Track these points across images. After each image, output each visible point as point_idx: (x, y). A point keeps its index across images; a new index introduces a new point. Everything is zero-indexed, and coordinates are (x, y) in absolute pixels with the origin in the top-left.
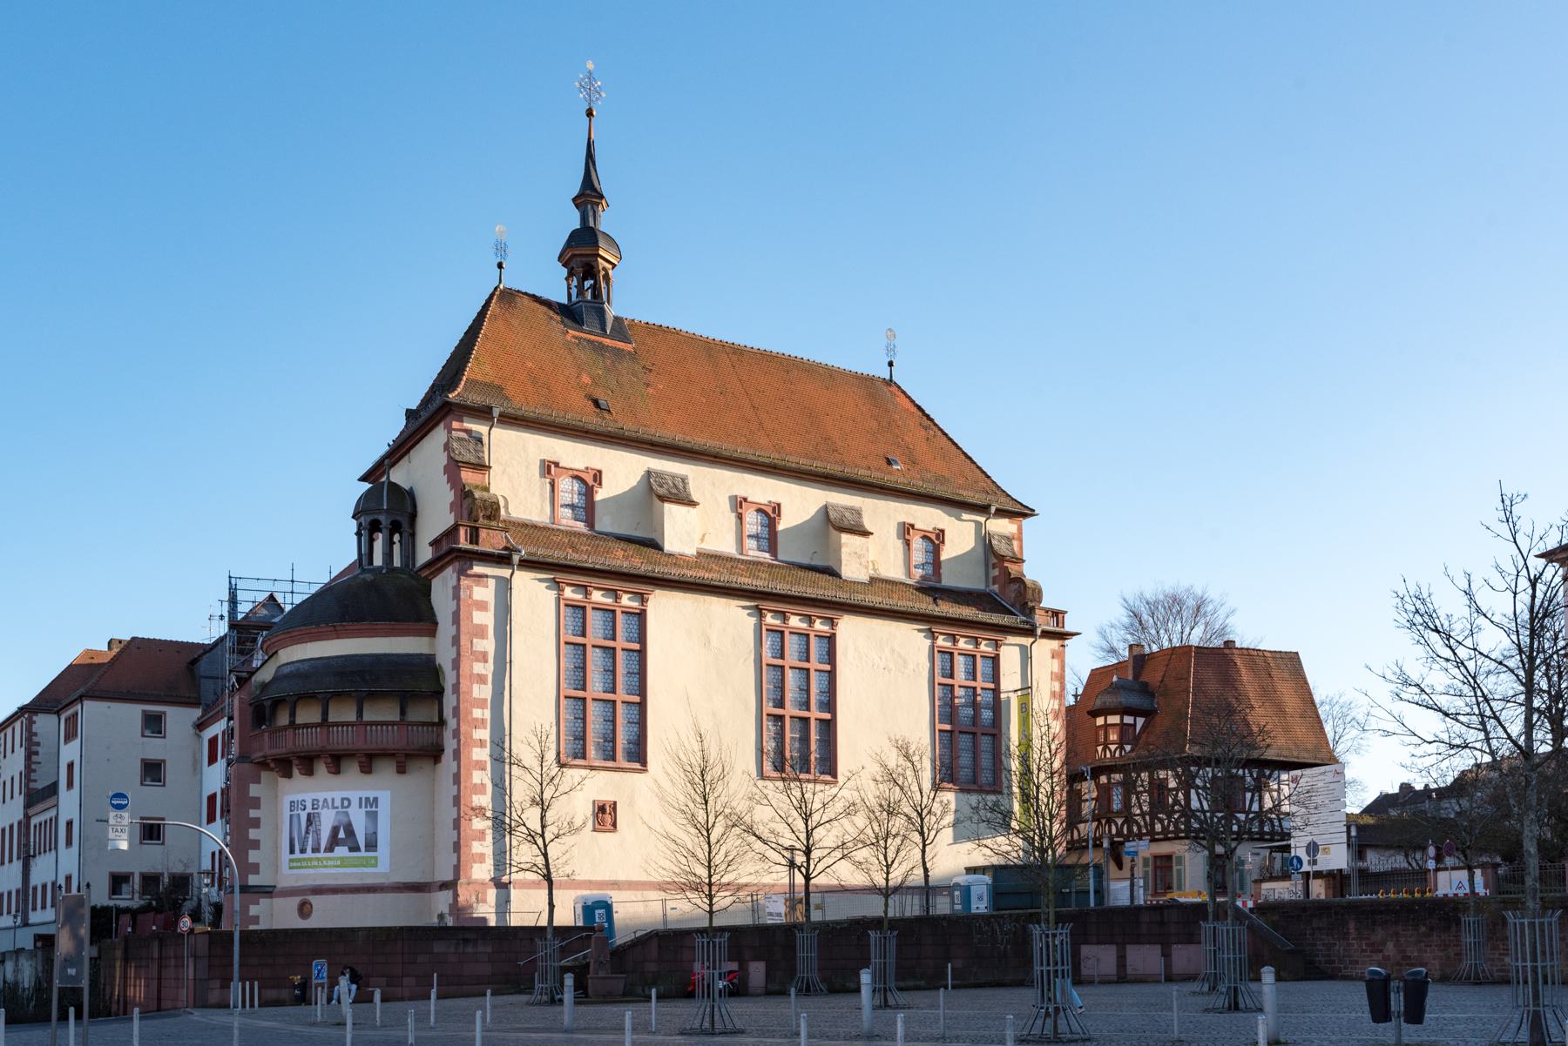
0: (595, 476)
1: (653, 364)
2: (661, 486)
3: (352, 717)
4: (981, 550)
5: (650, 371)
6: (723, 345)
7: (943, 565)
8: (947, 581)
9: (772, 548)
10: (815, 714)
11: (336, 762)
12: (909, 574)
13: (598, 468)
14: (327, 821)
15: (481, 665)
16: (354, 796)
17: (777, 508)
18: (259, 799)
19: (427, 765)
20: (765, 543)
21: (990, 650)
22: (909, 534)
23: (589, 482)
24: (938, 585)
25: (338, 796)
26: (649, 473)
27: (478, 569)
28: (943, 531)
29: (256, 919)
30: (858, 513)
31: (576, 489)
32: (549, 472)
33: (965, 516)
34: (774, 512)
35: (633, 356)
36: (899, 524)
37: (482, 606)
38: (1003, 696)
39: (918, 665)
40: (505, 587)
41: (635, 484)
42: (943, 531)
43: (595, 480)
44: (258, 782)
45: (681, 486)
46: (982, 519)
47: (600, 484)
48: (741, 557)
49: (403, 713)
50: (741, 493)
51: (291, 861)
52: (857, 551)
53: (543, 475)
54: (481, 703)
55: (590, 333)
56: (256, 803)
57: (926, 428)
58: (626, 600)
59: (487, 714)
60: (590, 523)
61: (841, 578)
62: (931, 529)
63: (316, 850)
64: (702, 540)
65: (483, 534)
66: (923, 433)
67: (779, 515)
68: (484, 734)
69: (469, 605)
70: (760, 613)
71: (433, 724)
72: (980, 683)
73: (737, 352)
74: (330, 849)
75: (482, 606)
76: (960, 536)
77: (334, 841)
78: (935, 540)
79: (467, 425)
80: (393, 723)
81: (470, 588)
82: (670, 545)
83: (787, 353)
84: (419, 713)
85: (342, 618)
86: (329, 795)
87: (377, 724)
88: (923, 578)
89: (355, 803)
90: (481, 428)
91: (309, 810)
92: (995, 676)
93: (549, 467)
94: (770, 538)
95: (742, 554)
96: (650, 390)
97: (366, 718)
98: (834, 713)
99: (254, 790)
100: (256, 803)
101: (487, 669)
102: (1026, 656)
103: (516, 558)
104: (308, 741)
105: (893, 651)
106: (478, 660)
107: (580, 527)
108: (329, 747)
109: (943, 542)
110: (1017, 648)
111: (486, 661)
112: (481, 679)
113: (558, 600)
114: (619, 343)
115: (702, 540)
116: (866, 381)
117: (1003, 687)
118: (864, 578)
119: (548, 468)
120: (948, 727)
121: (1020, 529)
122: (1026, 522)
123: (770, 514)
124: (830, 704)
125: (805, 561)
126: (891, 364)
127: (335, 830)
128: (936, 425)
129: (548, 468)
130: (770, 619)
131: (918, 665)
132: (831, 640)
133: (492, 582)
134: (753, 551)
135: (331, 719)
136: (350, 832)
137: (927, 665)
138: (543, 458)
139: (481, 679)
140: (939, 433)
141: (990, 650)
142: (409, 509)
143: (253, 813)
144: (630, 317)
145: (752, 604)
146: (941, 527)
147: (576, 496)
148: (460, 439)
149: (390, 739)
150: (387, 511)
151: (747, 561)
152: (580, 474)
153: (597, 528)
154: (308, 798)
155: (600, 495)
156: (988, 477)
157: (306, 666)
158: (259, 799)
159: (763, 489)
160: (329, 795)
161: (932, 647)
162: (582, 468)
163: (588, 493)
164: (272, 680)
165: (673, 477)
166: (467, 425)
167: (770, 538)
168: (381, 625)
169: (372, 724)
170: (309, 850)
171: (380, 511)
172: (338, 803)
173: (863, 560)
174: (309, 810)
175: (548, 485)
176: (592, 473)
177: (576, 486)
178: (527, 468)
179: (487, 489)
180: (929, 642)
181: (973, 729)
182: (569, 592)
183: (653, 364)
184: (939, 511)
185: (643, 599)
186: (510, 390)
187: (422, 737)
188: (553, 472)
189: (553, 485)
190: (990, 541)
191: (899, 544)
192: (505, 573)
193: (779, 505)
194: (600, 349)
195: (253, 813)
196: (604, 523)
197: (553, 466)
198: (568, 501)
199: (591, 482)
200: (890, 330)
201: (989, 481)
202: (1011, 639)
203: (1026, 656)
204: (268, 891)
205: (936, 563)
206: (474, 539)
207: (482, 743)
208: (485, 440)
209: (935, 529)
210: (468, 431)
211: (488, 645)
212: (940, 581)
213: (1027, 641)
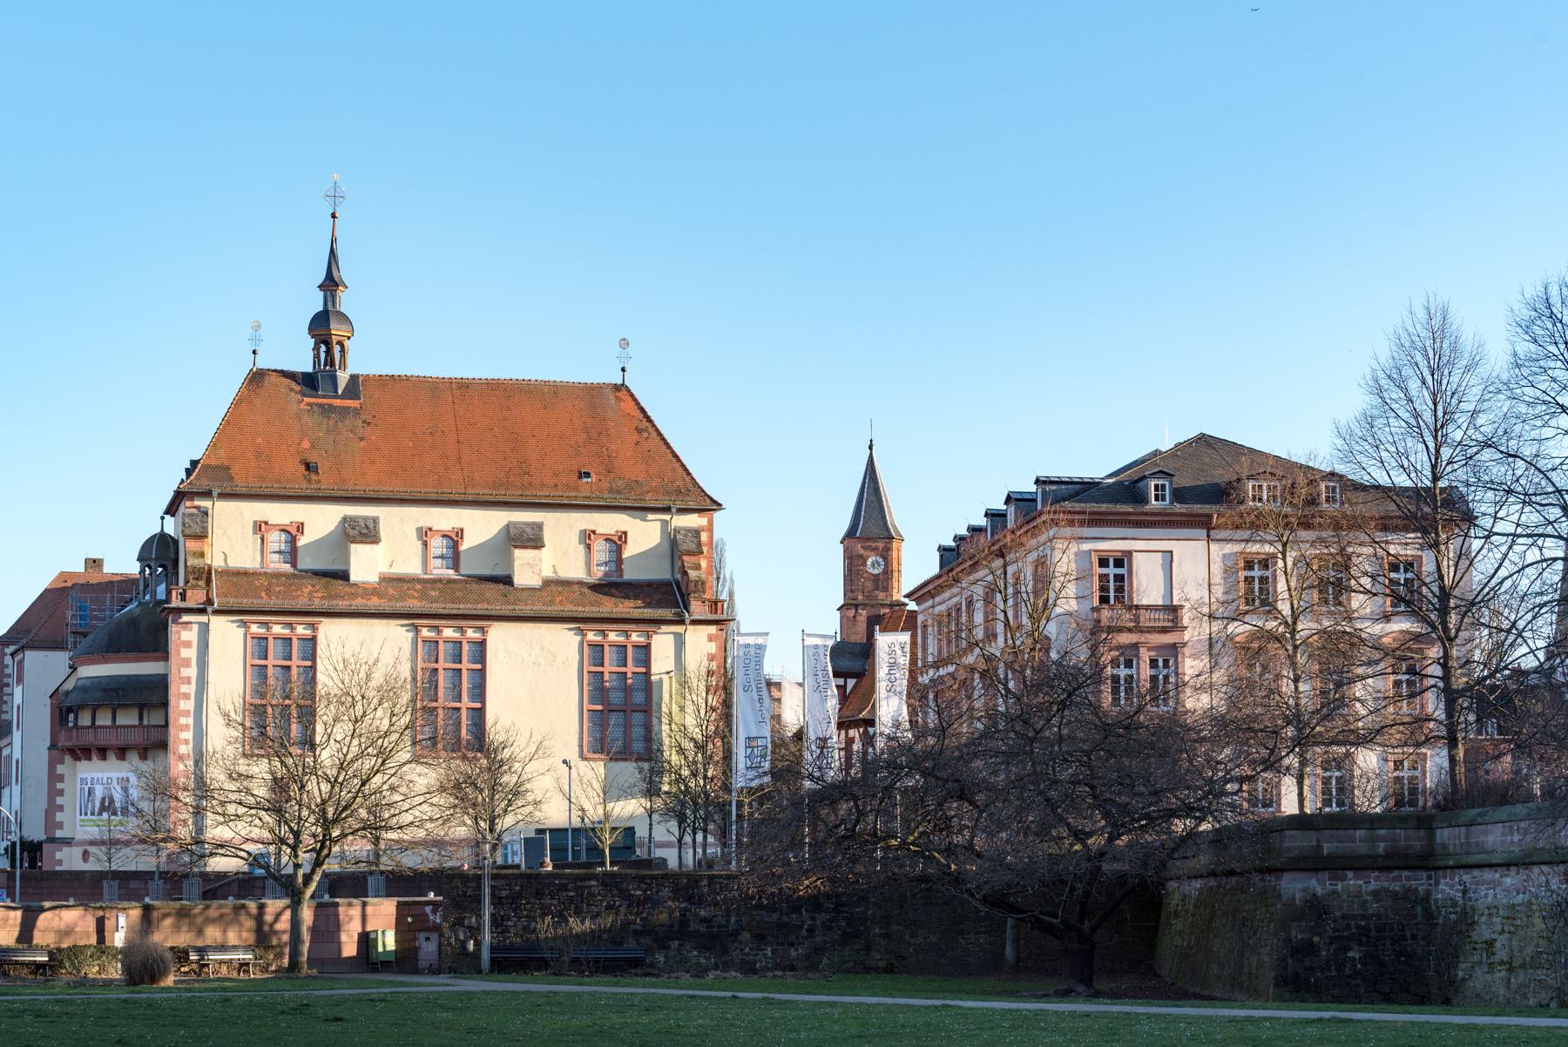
0: (298, 527)
1: (374, 417)
2: (354, 529)
3: (108, 722)
4: (667, 546)
5: (369, 424)
6: (450, 382)
7: (625, 562)
8: (629, 575)
9: (456, 567)
10: (466, 702)
11: (103, 753)
12: (589, 573)
13: (301, 521)
14: (99, 792)
15: (186, 686)
16: (115, 775)
17: (460, 533)
18: (63, 775)
19: (160, 753)
20: (450, 562)
21: (642, 639)
22: (590, 538)
23: (293, 533)
24: (619, 580)
25: (105, 775)
26: (345, 519)
27: (185, 618)
28: (625, 533)
29: (60, 862)
30: (539, 527)
31: (283, 539)
32: (260, 530)
33: (650, 516)
34: (457, 536)
35: (357, 412)
36: (581, 531)
37: (188, 644)
38: (653, 678)
39: (567, 658)
40: (205, 629)
41: (333, 528)
42: (625, 533)
43: (298, 531)
44: (63, 763)
45: (371, 526)
46: (667, 517)
47: (302, 533)
48: (425, 577)
49: (141, 719)
50: (425, 523)
51: (81, 820)
52: (531, 562)
53: (255, 533)
54: (186, 714)
55: (324, 397)
56: (61, 778)
57: (639, 430)
58: (300, 630)
59: (190, 721)
60: (294, 565)
61: (513, 586)
62: (613, 533)
63: (93, 814)
64: (391, 566)
65: (189, 593)
66: (635, 437)
67: (462, 538)
68: (188, 735)
69: (178, 645)
70: (416, 629)
71: (161, 726)
72: (631, 668)
73: (463, 386)
74: (100, 814)
75: (188, 644)
76: (643, 535)
77: (103, 809)
78: (618, 542)
79: (197, 503)
80: (134, 726)
81: (179, 633)
82: (354, 577)
83: (514, 377)
84: (153, 718)
85: (108, 651)
86: (100, 775)
87: (124, 727)
88: (606, 574)
89: (115, 782)
90: (205, 504)
91: (89, 785)
92: (646, 662)
93: (260, 525)
94: (454, 557)
95: (426, 573)
96: (363, 444)
97: (118, 723)
98: (483, 702)
99: (60, 769)
100: (61, 778)
101: (191, 689)
102: (680, 642)
103: (210, 609)
104: (88, 739)
105: (542, 648)
106: (184, 683)
107: (287, 568)
108: (96, 743)
109: (625, 542)
110: (672, 636)
111: (190, 683)
112: (186, 696)
113: (245, 635)
114: (348, 401)
115: (391, 566)
116: (592, 392)
117: (654, 669)
118: (536, 582)
119: (260, 527)
120: (600, 707)
121: (711, 523)
122: (717, 516)
123: (454, 538)
124: (479, 691)
125: (487, 572)
126: (623, 370)
127: (103, 799)
128: (654, 426)
129: (260, 527)
130: (425, 632)
131: (567, 658)
132: (481, 645)
133: (195, 627)
134: (440, 570)
135: (97, 723)
136: (112, 801)
137: (577, 657)
138: (255, 519)
139: (186, 696)
140: (654, 434)
141: (642, 639)
142: (172, 556)
143: (59, 786)
144: (365, 373)
145: (411, 622)
146: (623, 529)
147: (283, 545)
148: (191, 515)
149: (135, 737)
150: (155, 559)
151: (430, 579)
152: (286, 528)
153: (299, 567)
154: (89, 776)
155: (302, 541)
156: (689, 474)
157: (88, 682)
158: (63, 775)
159: (444, 518)
160: (100, 775)
161: (581, 644)
162: (288, 523)
163: (293, 541)
164: (74, 688)
165: (366, 519)
166: (197, 503)
167: (454, 557)
168: (130, 655)
169: (121, 727)
170: (89, 814)
171: (151, 559)
172: (105, 781)
173: (536, 570)
174: (89, 785)
175: (259, 540)
176: (295, 526)
177: (283, 536)
178: (243, 529)
179: (202, 555)
180: (579, 638)
181: (623, 708)
182: (254, 628)
183: (374, 417)
184: (624, 516)
185: (313, 627)
186: (236, 470)
187: (155, 736)
188: (263, 529)
189: (262, 539)
190: (675, 536)
191: (581, 548)
192: (203, 619)
193: (462, 530)
194: (327, 410)
195: (59, 786)
196: (305, 563)
197: (263, 525)
198: (277, 549)
199: (294, 533)
200: (624, 340)
201: (688, 479)
202: (665, 628)
203: (680, 642)
204: (68, 842)
205: (619, 561)
206: (183, 597)
207: (186, 742)
208: (210, 513)
209: (617, 532)
210: (197, 508)
211: (192, 672)
212: (622, 576)
213: (679, 629)
